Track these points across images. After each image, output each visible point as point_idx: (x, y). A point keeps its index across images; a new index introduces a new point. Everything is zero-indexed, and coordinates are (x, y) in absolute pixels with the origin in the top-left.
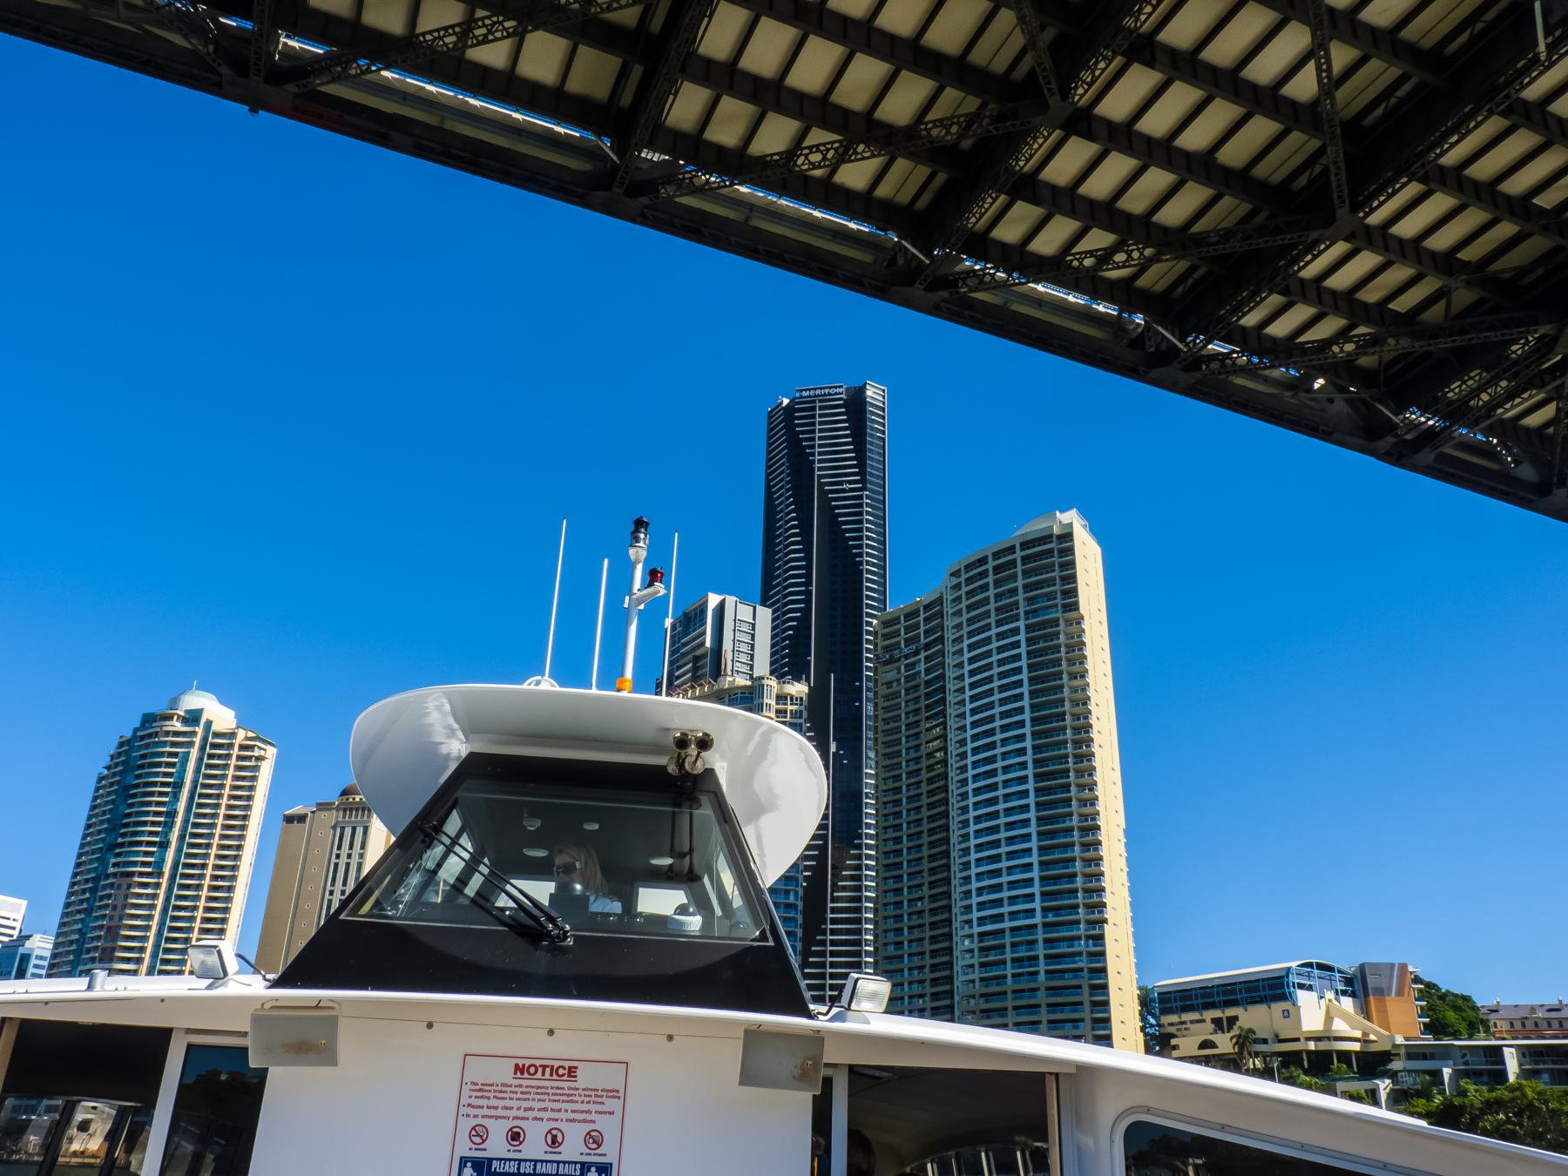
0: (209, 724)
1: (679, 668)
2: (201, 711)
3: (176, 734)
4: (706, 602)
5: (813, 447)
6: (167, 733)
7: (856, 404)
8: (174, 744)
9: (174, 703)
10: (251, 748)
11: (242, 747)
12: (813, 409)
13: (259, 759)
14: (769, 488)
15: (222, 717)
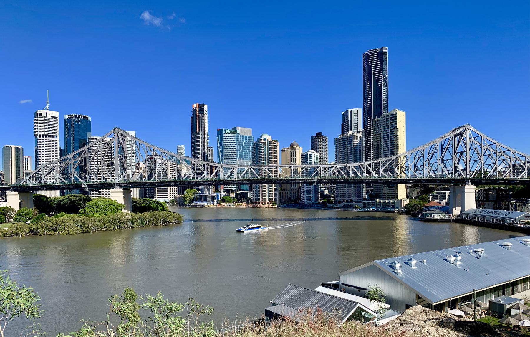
0: (268, 140)
1: (345, 122)
2: (266, 138)
3: (263, 142)
4: (348, 111)
5: (371, 65)
6: (262, 142)
7: (381, 54)
8: (263, 144)
9: (261, 137)
10: (275, 144)
11: (274, 144)
12: (371, 55)
13: (277, 145)
14: (364, 74)
15: (269, 138)
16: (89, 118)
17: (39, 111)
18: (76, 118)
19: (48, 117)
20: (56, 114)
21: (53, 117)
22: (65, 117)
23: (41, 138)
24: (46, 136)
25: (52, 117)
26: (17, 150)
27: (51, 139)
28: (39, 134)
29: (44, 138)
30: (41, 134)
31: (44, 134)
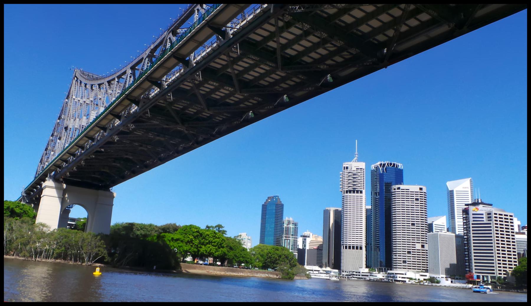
16: (400, 166)
17: (345, 165)
18: (381, 166)
19: (352, 170)
20: (362, 165)
21: (358, 169)
22: (373, 167)
23: (346, 195)
24: (350, 191)
25: (357, 169)
26: (337, 213)
27: (356, 194)
28: (343, 190)
29: (349, 194)
30: (345, 190)
31: (347, 189)
